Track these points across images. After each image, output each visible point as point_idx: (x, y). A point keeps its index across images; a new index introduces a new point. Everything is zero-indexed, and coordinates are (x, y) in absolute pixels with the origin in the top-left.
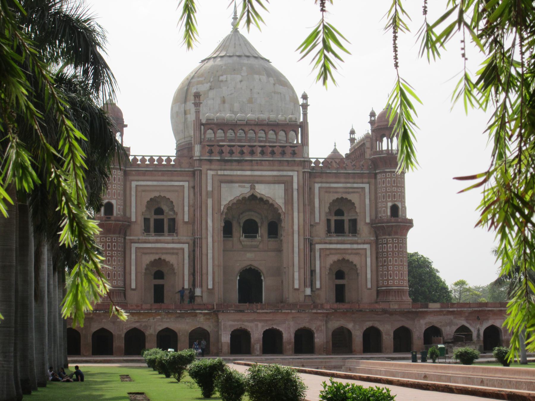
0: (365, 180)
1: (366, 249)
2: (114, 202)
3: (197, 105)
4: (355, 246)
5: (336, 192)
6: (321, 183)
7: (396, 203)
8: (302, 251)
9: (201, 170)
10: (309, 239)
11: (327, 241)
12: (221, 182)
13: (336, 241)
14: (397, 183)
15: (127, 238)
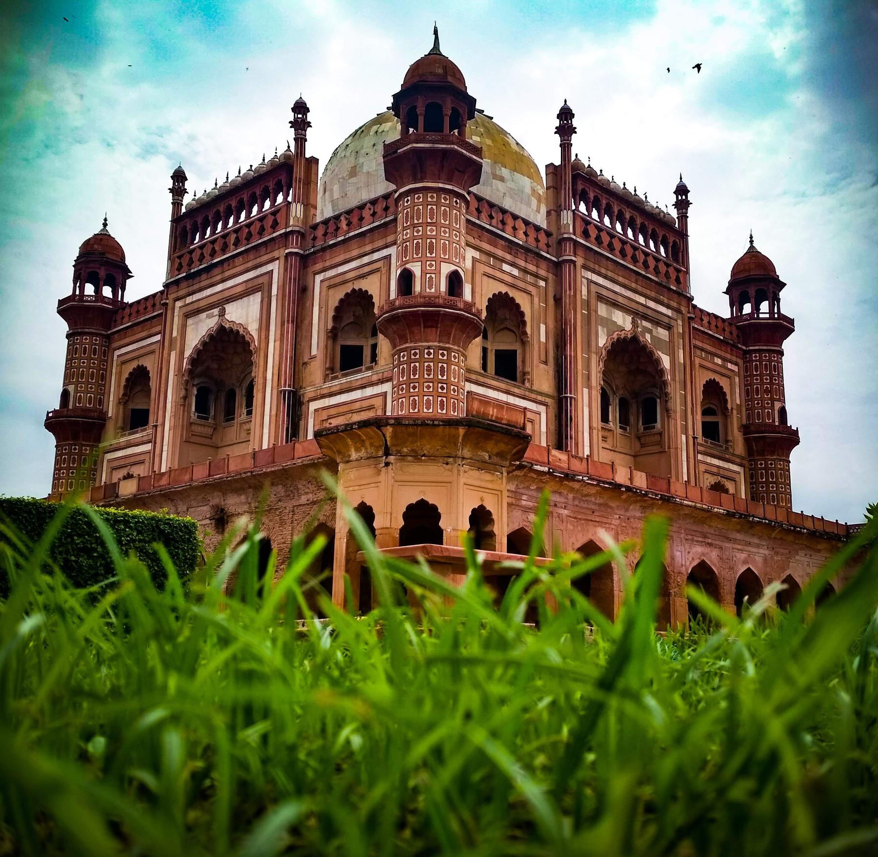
0: (390, 239)
1: (385, 395)
2: (71, 388)
3: (178, 191)
4: (369, 391)
5: (345, 282)
6: (324, 270)
7: (408, 266)
8: (274, 418)
9: (166, 304)
10: (285, 391)
11: (325, 391)
12: (187, 316)
13: (337, 388)
14: (413, 218)
15: (101, 445)
